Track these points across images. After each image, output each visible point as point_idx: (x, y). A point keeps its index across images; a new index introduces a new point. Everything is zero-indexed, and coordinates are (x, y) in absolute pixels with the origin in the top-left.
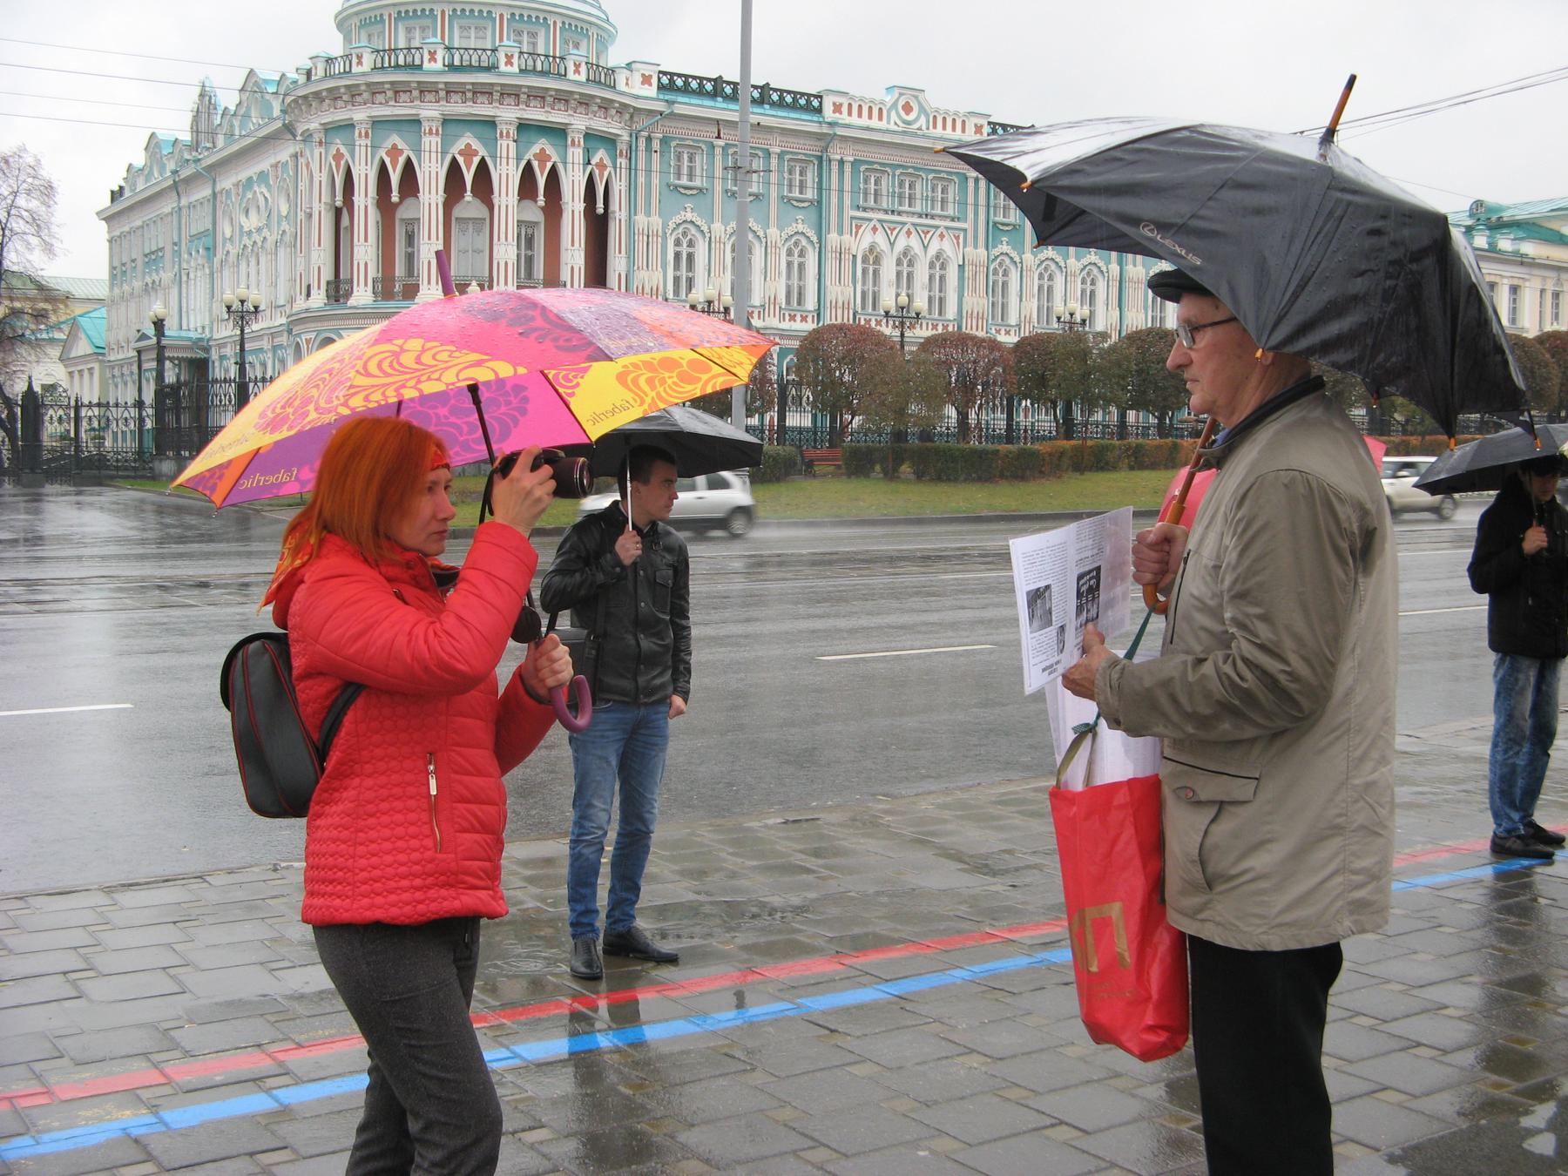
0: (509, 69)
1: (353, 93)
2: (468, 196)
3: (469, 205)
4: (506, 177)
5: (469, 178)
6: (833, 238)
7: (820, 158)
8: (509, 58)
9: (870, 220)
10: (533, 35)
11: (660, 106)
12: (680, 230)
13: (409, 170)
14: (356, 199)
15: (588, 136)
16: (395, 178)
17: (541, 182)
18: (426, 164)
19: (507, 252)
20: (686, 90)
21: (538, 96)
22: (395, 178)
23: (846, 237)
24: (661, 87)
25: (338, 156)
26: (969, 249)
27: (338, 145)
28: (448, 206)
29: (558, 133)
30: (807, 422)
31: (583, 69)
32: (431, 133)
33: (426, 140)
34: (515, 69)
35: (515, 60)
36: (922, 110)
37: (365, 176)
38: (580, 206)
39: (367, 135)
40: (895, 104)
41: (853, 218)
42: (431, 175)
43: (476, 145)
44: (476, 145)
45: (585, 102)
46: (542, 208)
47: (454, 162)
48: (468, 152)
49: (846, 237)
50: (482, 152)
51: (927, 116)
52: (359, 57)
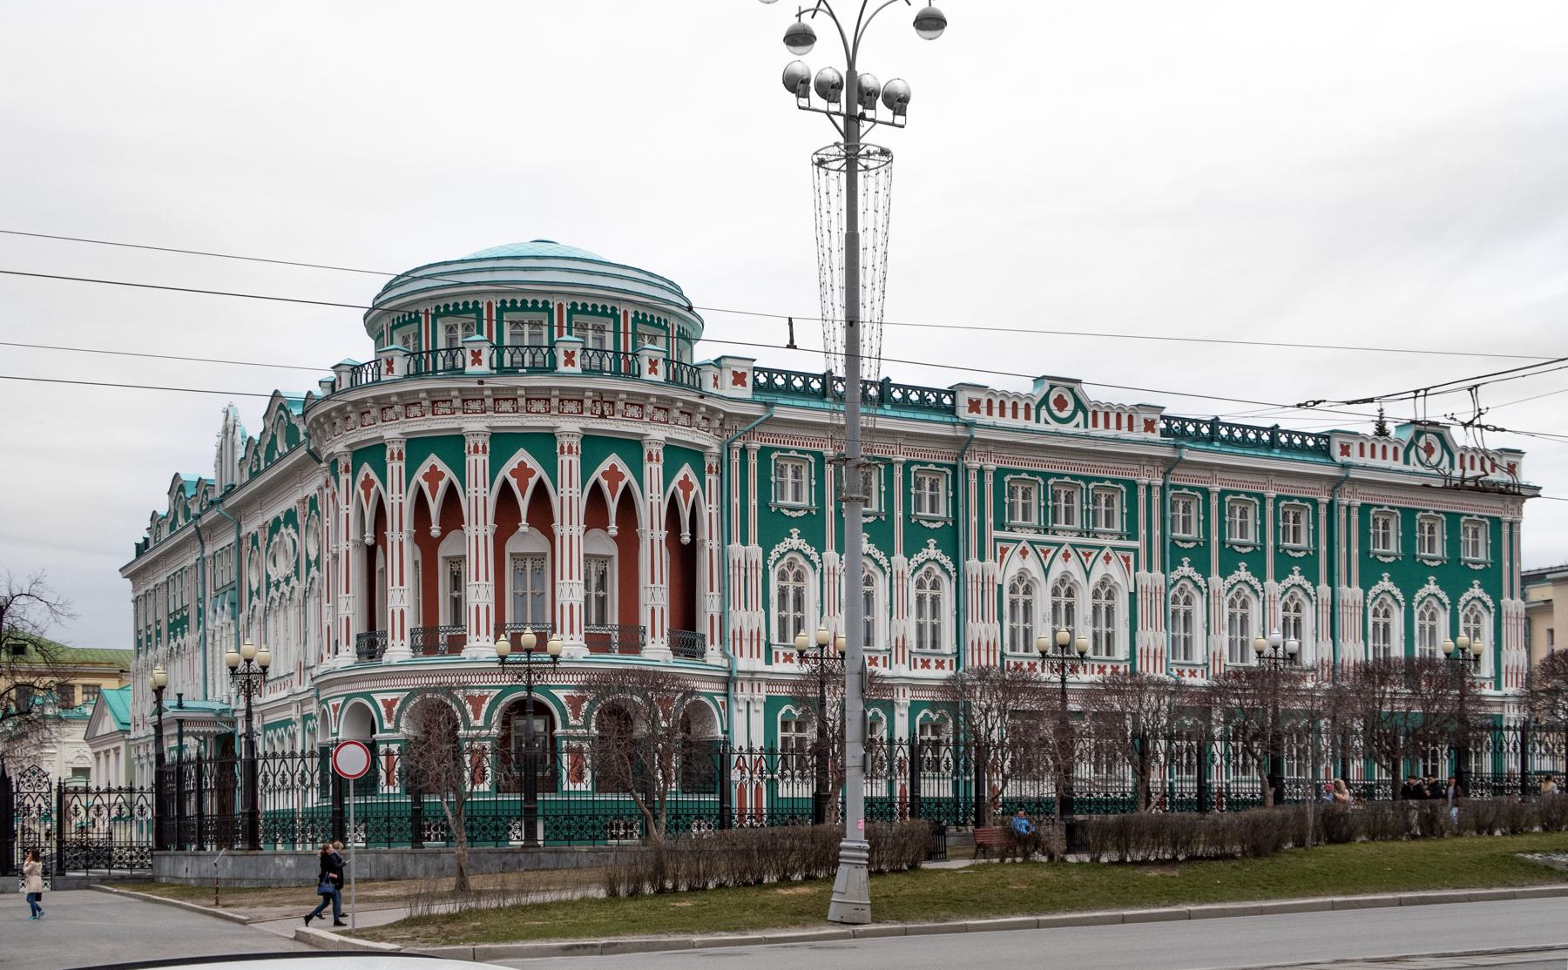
0: (569, 369)
1: (384, 404)
2: (524, 526)
3: (525, 539)
4: (569, 496)
5: (524, 504)
6: (973, 565)
7: (954, 468)
8: (569, 357)
9: (1018, 542)
10: (601, 329)
11: (755, 410)
12: (785, 560)
13: (451, 496)
14: (388, 533)
15: (667, 448)
16: (434, 507)
17: (613, 507)
18: (471, 489)
19: (571, 592)
20: (788, 390)
21: (605, 402)
22: (434, 507)
23: (989, 562)
24: (757, 387)
25: (368, 484)
26: (1143, 572)
27: (367, 469)
29: (632, 448)
30: (947, 792)
31: (661, 367)
32: (476, 450)
33: (471, 459)
34: (577, 369)
35: (577, 359)
36: (1079, 405)
38: (661, 534)
39: (400, 454)
40: (1044, 401)
41: (996, 540)
42: (479, 498)
45: (665, 405)
46: (615, 538)
47: (506, 483)
49: (989, 562)
50: (540, 472)
51: (1085, 412)
52: (390, 363)
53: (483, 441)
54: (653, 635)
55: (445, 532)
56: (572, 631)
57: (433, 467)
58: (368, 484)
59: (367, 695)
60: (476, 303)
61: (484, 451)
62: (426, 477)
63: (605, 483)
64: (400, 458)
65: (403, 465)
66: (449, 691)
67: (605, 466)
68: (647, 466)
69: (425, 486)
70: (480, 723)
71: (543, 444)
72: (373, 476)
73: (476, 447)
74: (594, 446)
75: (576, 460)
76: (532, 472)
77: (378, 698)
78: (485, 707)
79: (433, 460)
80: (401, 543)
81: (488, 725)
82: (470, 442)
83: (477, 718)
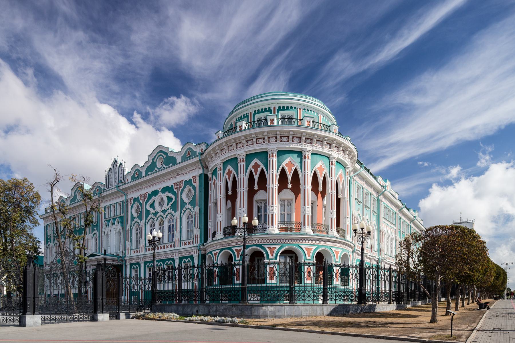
5: (256, 178)
18: (239, 175)
43: (259, 163)
44: (259, 163)
50: (262, 166)
65: (222, 172)
71: (264, 155)
76: (259, 166)
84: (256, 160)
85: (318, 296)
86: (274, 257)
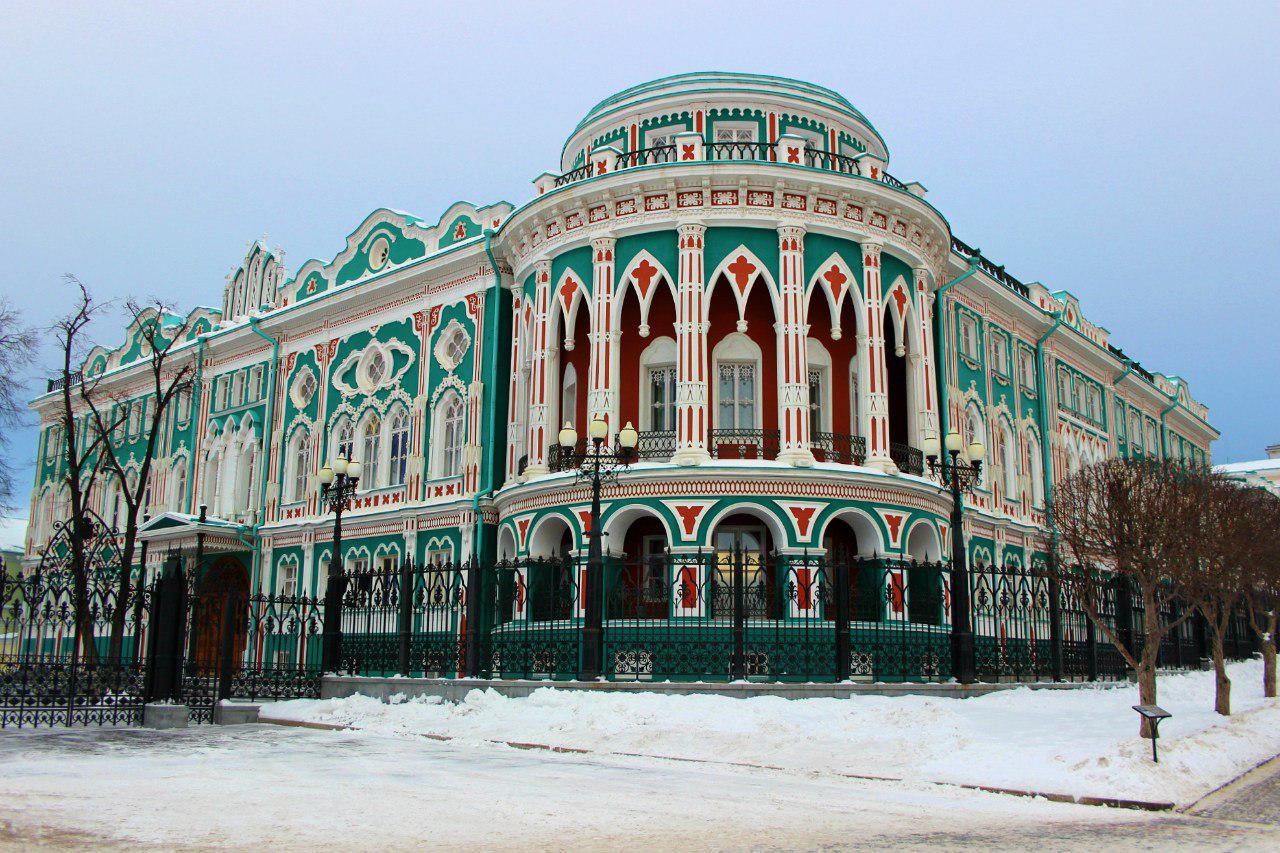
2: (742, 325)
3: (740, 347)
5: (742, 301)
13: (663, 294)
14: (592, 337)
15: (884, 256)
16: (645, 304)
22: (645, 304)
27: (569, 273)
28: (715, 336)
29: (851, 249)
33: (684, 253)
37: (606, 306)
38: (879, 342)
39: (608, 257)
42: (692, 295)
47: (722, 277)
48: (742, 268)
50: (761, 268)
53: (698, 234)
54: (874, 447)
55: (655, 333)
56: (799, 439)
57: (645, 263)
58: (570, 287)
59: (564, 510)
60: (685, 114)
61: (699, 246)
62: (635, 273)
63: (827, 285)
64: (608, 257)
65: (612, 265)
66: (656, 503)
67: (826, 267)
68: (866, 269)
69: (635, 282)
70: (693, 537)
71: (765, 240)
72: (575, 279)
73: (691, 243)
74: (817, 245)
75: (799, 256)
76: (752, 268)
77: (576, 511)
78: (698, 519)
79: (644, 255)
80: (607, 344)
81: (701, 540)
82: (684, 235)
83: (689, 531)
84: (742, 251)
85: (917, 660)
86: (808, 538)
